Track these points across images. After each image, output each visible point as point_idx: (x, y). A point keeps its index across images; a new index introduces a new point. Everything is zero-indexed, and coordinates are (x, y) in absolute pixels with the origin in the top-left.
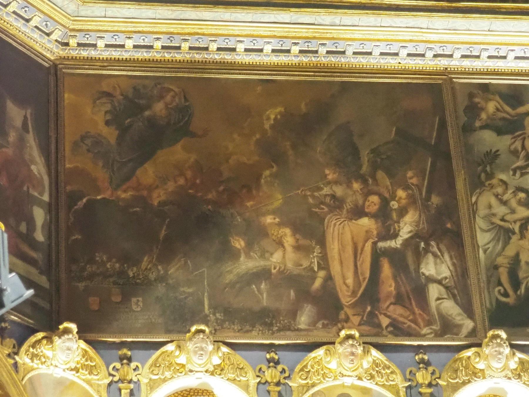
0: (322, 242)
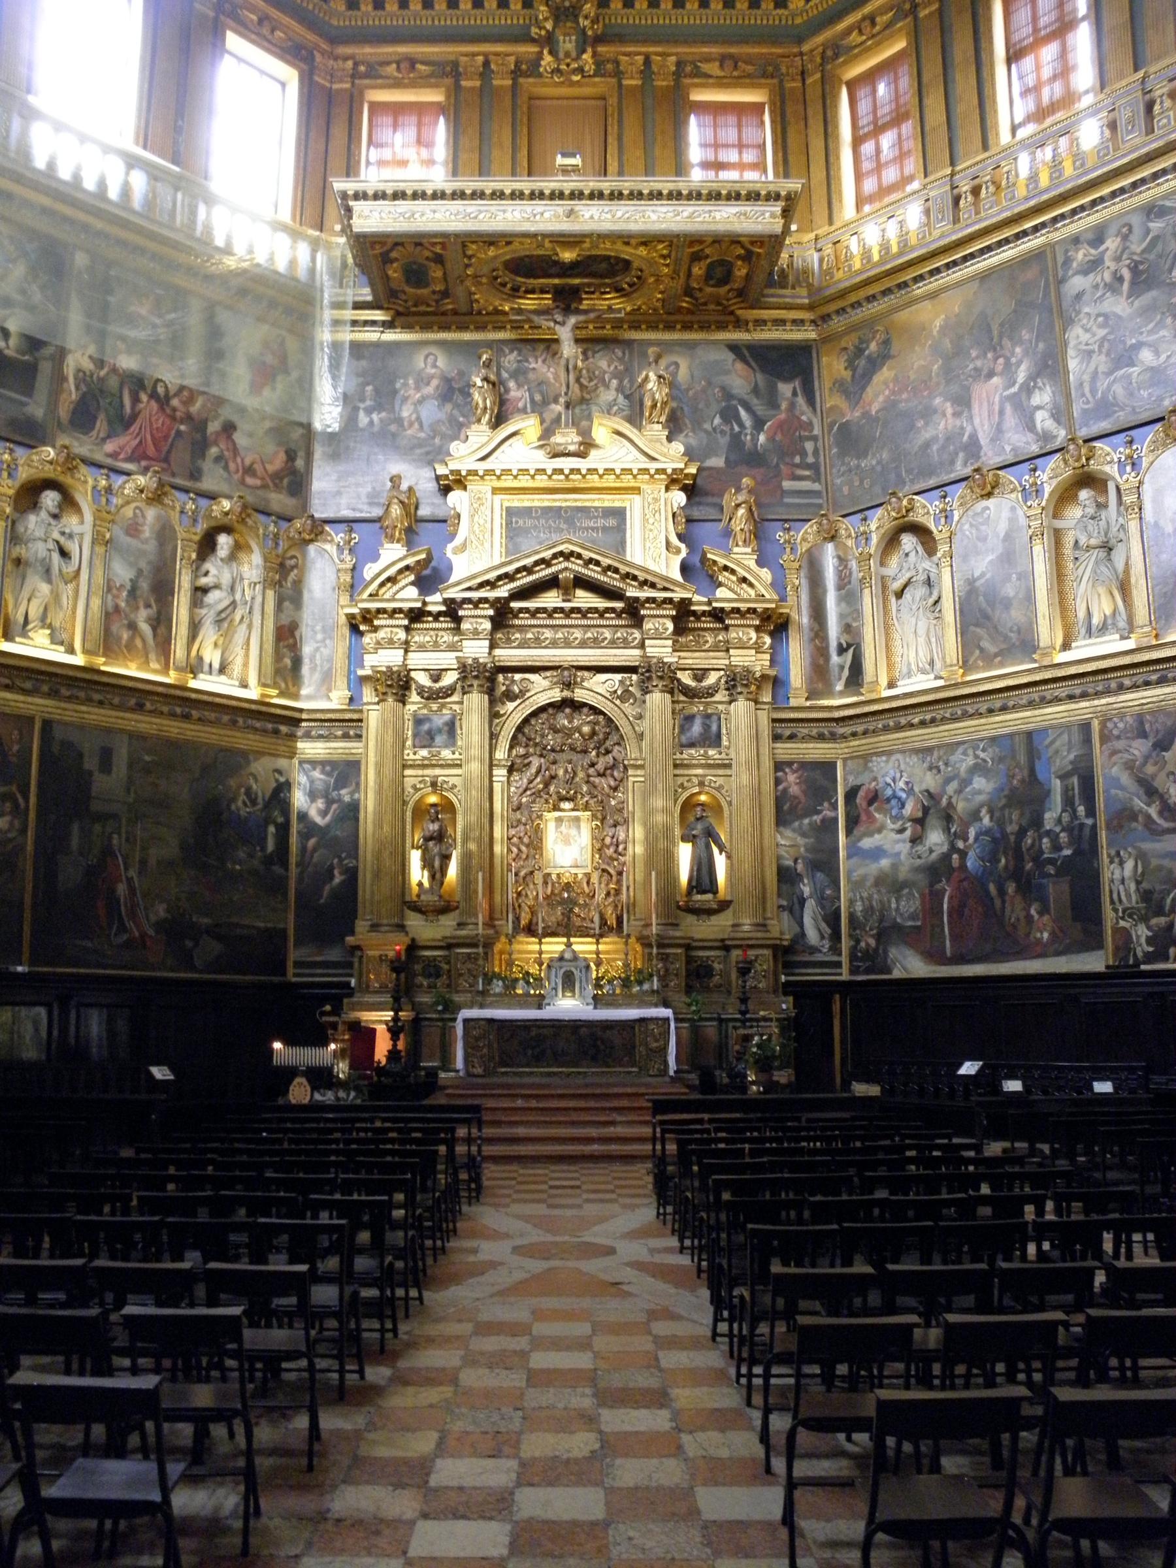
0: (968, 405)
